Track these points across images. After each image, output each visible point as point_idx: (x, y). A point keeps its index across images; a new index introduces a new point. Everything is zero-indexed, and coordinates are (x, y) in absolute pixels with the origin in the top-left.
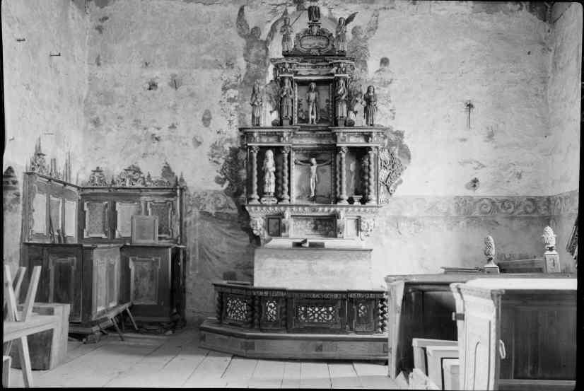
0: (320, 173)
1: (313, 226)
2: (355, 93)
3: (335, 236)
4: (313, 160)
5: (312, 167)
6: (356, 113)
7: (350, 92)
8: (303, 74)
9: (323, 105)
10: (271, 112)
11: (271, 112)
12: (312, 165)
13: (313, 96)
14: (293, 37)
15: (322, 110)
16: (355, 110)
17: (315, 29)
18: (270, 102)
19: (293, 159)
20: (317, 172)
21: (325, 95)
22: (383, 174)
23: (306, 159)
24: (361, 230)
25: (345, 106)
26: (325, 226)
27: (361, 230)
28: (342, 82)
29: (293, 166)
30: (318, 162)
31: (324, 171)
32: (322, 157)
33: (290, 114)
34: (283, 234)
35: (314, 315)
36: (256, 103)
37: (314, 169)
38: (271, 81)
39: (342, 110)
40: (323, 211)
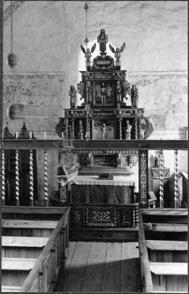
0: (108, 131)
1: (104, 160)
2: (126, 88)
3: (116, 166)
4: (104, 125)
5: (104, 128)
6: (127, 99)
7: (123, 87)
8: (98, 77)
9: (109, 94)
10: (81, 99)
11: (81, 99)
12: (104, 127)
13: (103, 90)
14: (92, 59)
15: (109, 97)
16: (126, 97)
17: (104, 57)
18: (80, 93)
19: (93, 124)
20: (106, 131)
21: (109, 90)
22: (142, 132)
23: (102, 123)
24: (130, 163)
25: (120, 96)
26: (111, 160)
27: (130, 163)
28: (119, 82)
29: (93, 128)
30: (107, 125)
31: (110, 130)
32: (109, 122)
33: (91, 100)
34: (88, 165)
35: (100, 216)
36: (72, 95)
37: (104, 129)
38: (81, 82)
39: (119, 97)
40: (109, 152)
